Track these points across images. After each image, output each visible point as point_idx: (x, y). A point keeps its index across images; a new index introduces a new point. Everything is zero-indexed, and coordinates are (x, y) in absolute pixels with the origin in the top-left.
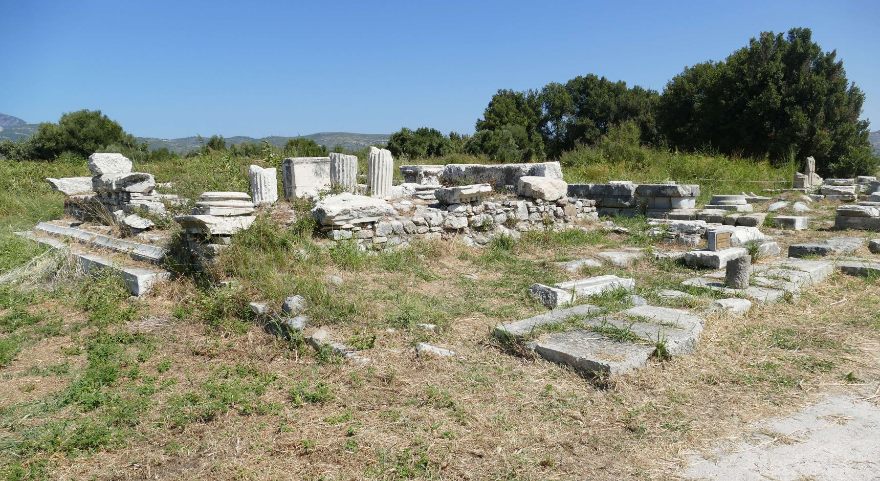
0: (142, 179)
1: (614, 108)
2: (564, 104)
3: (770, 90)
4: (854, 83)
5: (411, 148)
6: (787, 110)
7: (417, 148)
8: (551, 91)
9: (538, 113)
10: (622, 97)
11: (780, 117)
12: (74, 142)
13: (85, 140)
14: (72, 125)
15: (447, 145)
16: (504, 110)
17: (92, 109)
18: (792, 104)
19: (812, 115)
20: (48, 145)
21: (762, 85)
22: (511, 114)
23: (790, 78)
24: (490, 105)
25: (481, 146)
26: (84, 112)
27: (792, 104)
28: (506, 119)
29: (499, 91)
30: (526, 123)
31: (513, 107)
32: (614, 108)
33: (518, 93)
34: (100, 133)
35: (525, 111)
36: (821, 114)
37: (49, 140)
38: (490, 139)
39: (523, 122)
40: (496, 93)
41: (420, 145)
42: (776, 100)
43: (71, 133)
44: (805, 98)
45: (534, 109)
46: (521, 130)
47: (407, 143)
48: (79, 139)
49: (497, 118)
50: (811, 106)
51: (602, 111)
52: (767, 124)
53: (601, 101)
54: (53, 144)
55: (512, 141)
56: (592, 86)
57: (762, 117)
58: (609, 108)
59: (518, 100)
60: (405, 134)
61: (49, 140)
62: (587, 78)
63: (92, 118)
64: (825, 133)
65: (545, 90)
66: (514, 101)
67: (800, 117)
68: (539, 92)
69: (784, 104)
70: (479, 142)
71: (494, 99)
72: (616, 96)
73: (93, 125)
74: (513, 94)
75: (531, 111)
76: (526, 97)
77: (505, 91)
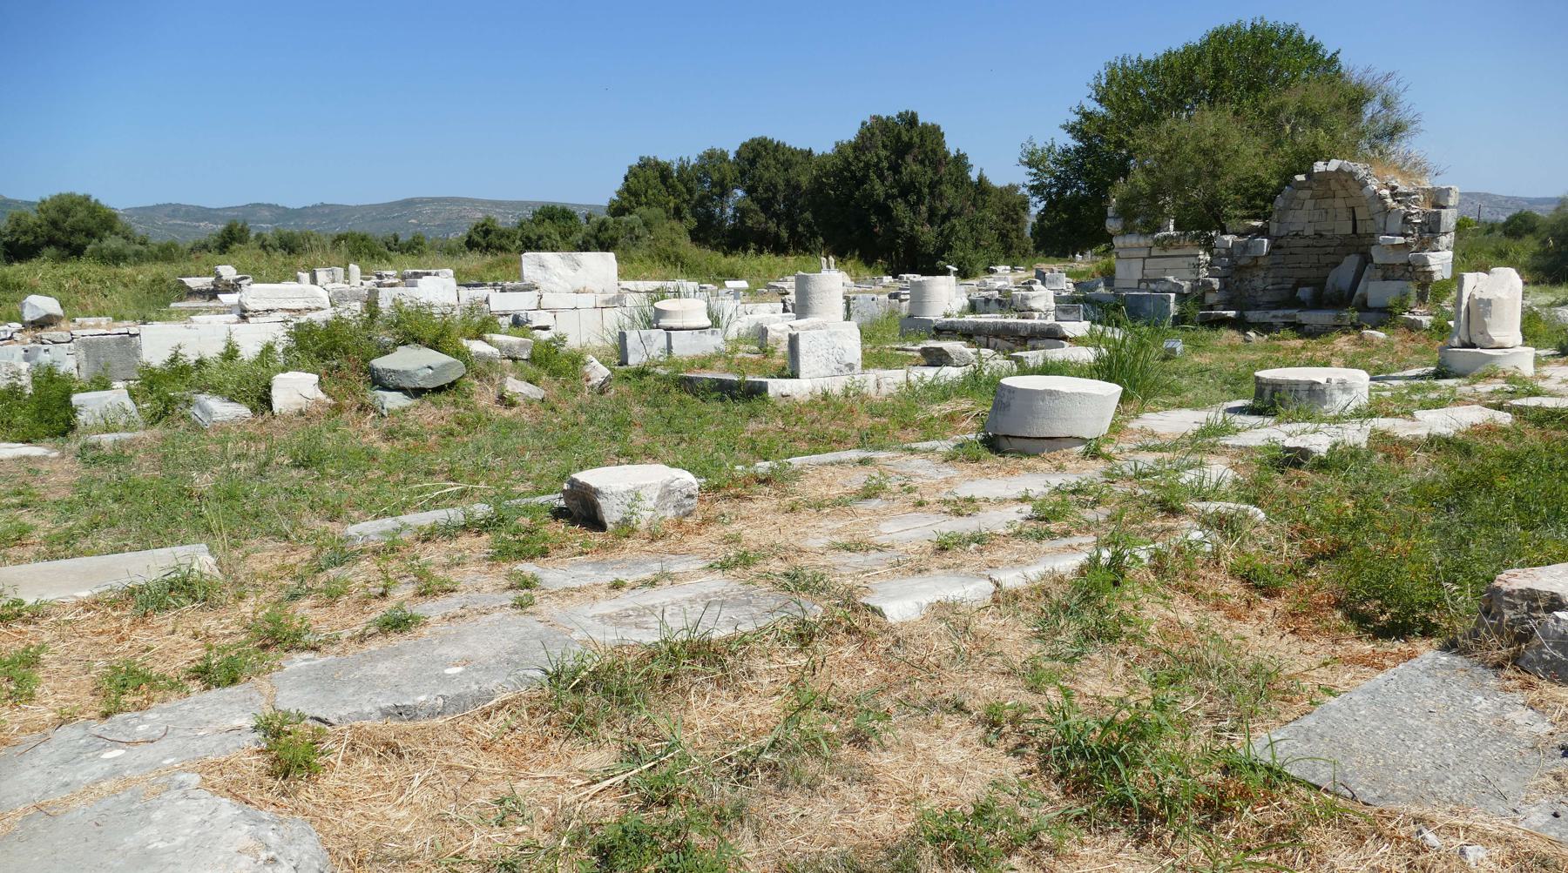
0: (246, 278)
2: (723, 179)
3: (872, 181)
4: (982, 170)
5: (498, 242)
11: (884, 211)
12: (58, 235)
13: (72, 233)
14: (53, 214)
15: (549, 237)
16: (643, 186)
17: (80, 192)
18: (893, 197)
19: (914, 207)
20: (23, 239)
21: (865, 178)
23: (895, 168)
25: (596, 237)
26: (70, 196)
27: (893, 197)
29: (641, 159)
30: (672, 205)
33: (665, 163)
34: (92, 223)
35: (673, 187)
36: (923, 209)
37: (25, 233)
38: (607, 229)
39: (668, 203)
40: (635, 162)
41: (508, 237)
42: (879, 190)
43: (54, 224)
44: (907, 190)
45: (685, 186)
47: (492, 236)
48: (64, 231)
49: (632, 198)
50: (913, 198)
51: (766, 190)
52: (874, 219)
53: (767, 175)
54: (30, 238)
57: (868, 210)
59: (664, 172)
60: (489, 223)
61: (25, 233)
63: (80, 204)
64: (927, 228)
65: (701, 157)
67: (900, 209)
69: (888, 196)
71: (630, 172)
72: (786, 170)
73: (81, 214)
74: (657, 164)
75: (681, 187)
76: (675, 168)
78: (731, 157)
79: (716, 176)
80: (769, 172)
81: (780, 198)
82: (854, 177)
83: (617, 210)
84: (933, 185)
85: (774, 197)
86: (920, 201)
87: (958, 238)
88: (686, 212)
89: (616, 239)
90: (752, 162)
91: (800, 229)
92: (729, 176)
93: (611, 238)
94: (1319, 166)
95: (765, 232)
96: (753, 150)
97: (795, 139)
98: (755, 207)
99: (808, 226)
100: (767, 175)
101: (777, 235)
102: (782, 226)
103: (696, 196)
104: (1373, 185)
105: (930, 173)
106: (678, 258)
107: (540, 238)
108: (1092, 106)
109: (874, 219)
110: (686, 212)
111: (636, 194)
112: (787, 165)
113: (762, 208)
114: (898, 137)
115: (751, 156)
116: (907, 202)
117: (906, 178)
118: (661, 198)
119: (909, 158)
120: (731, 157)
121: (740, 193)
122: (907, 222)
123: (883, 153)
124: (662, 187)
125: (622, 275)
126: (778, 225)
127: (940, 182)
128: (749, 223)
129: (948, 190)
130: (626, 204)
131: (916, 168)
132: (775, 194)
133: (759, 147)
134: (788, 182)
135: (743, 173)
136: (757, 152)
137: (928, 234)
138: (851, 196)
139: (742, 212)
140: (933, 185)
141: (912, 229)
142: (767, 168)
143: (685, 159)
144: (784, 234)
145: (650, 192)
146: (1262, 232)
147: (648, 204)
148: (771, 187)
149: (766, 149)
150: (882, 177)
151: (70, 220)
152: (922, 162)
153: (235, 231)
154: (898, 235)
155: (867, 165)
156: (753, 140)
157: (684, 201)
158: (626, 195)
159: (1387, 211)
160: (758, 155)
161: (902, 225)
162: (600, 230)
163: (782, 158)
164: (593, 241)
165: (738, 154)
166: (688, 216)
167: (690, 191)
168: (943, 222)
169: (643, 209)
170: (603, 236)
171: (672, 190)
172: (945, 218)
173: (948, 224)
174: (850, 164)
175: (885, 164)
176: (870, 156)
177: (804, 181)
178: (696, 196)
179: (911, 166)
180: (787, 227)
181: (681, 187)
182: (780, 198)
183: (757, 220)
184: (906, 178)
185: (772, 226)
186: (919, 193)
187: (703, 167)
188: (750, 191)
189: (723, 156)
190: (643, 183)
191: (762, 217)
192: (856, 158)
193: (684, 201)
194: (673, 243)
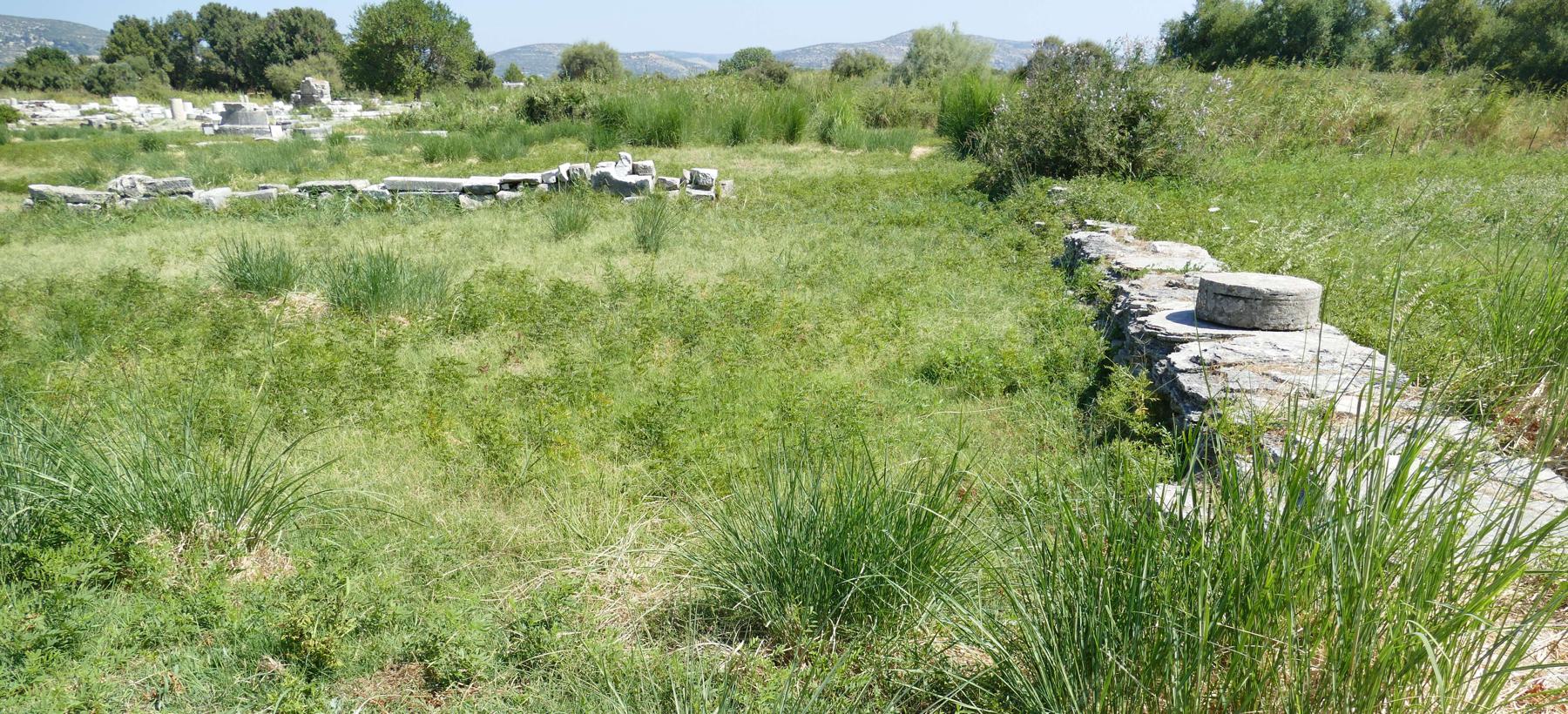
2: (190, 35)
7: (32, 82)
8: (180, 18)
23: (290, 42)
25: (97, 78)
30: (152, 53)
32: (234, 42)
35: (150, 39)
38: (105, 73)
39: (149, 52)
51: (223, 45)
58: (229, 43)
59: (142, 28)
68: (164, 22)
70: (96, 74)
71: (115, 27)
72: (236, 30)
74: (137, 21)
78: (195, 18)
79: (184, 33)
80: (223, 31)
82: (266, 47)
85: (229, 50)
88: (165, 59)
89: (114, 80)
90: (212, 22)
92: (195, 32)
98: (216, 57)
102: (239, 71)
103: (170, 47)
106: (158, 94)
110: (165, 59)
111: (122, 45)
112: (236, 27)
113: (221, 57)
114: (289, 24)
115: (210, 17)
117: (297, 49)
118: (142, 48)
119: (298, 36)
120: (195, 18)
121: (205, 44)
123: (281, 33)
124: (142, 40)
126: (235, 70)
130: (115, 52)
131: (301, 42)
132: (230, 48)
133: (215, 12)
135: (205, 30)
139: (207, 61)
145: (133, 44)
147: (133, 53)
149: (221, 12)
150: (282, 47)
152: (306, 39)
155: (272, 40)
156: (210, 4)
158: (114, 45)
160: (215, 16)
162: (100, 73)
163: (233, 20)
165: (200, 15)
166: (167, 62)
167: (165, 43)
169: (129, 57)
170: (103, 78)
171: (150, 42)
175: (283, 40)
176: (272, 35)
178: (170, 47)
179: (299, 42)
180: (243, 72)
181: (157, 40)
183: (218, 66)
185: (231, 71)
187: (173, 24)
188: (213, 43)
189: (188, 16)
190: (127, 37)
191: (222, 64)
194: (155, 87)
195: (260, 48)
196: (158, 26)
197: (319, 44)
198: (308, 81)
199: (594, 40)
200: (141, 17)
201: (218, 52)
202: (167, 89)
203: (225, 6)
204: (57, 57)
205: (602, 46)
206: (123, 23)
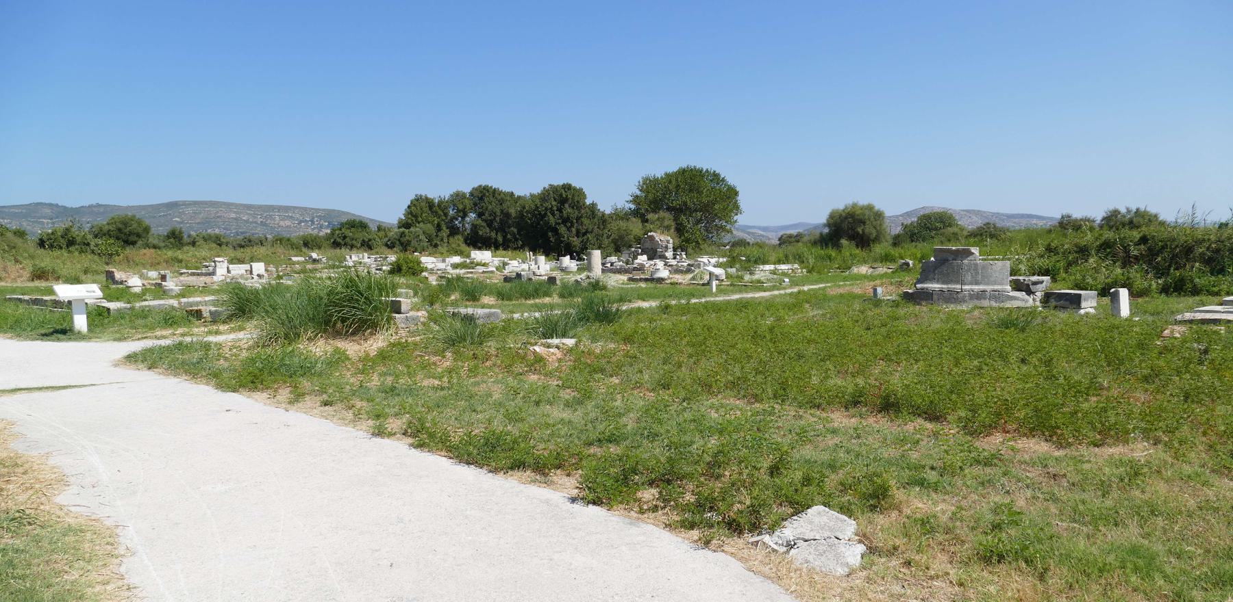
1: (498, 214)
6: (557, 226)
7: (354, 242)
8: (458, 196)
9: (446, 215)
10: (505, 206)
11: (555, 231)
13: (129, 235)
16: (419, 212)
18: (559, 224)
19: (569, 229)
21: (546, 214)
22: (424, 215)
23: (560, 210)
24: (409, 207)
25: (399, 240)
27: (559, 224)
28: (420, 219)
29: (416, 196)
30: (436, 222)
31: (426, 209)
32: (498, 214)
34: (140, 230)
35: (436, 212)
38: (405, 236)
39: (434, 221)
40: (413, 197)
41: (356, 240)
44: (565, 221)
45: (443, 211)
46: (430, 228)
47: (347, 239)
48: (125, 234)
51: (490, 215)
52: (550, 234)
53: (490, 207)
55: (422, 237)
56: (487, 194)
59: (430, 204)
62: (484, 188)
65: (452, 196)
66: (427, 205)
67: (562, 229)
68: (446, 199)
69: (557, 224)
71: (411, 203)
72: (501, 204)
73: (135, 226)
74: (427, 198)
75: (440, 213)
76: (437, 201)
77: (421, 196)
80: (493, 206)
81: (498, 219)
82: (540, 214)
83: (405, 225)
84: (578, 219)
85: (495, 219)
86: (572, 226)
87: (590, 244)
90: (481, 199)
91: (509, 236)
93: (408, 241)
94: (649, 234)
95: (490, 238)
96: (481, 192)
97: (504, 186)
98: (484, 224)
99: (513, 235)
100: (490, 207)
101: (496, 239)
104: (657, 239)
105: (577, 212)
107: (370, 240)
108: (638, 193)
109: (550, 234)
111: (416, 217)
112: (501, 202)
114: (561, 195)
115: (480, 195)
116: (565, 226)
117: (565, 215)
119: (567, 205)
122: (565, 235)
123: (554, 203)
125: (492, 257)
127: (581, 217)
128: (481, 233)
129: (586, 221)
130: (410, 221)
131: (570, 210)
134: (502, 211)
135: (475, 205)
136: (483, 195)
137: (576, 241)
138: (539, 224)
139: (475, 227)
140: (578, 219)
141: (569, 239)
142: (490, 203)
143: (442, 197)
144: (500, 239)
146: (640, 248)
148: (493, 214)
149: (488, 191)
150: (553, 215)
151: (128, 229)
152: (573, 207)
153: (177, 233)
154: (562, 242)
155: (546, 209)
156: (480, 186)
157: (443, 220)
158: (410, 216)
159: (659, 244)
160: (484, 195)
161: (564, 237)
162: (401, 237)
163: (499, 198)
164: (398, 242)
166: (444, 228)
168: (583, 236)
169: (422, 225)
170: (403, 240)
172: (585, 234)
173: (585, 237)
174: (538, 207)
175: (555, 208)
176: (547, 205)
177: (512, 211)
179: (567, 210)
182: (498, 219)
183: (484, 231)
184: (565, 215)
185: (493, 234)
186: (572, 222)
188: (480, 215)
189: (464, 195)
191: (488, 230)
192: (542, 205)
193: (443, 220)
195: (534, 215)
196: (441, 202)
197: (583, 211)
198: (652, 238)
199: (863, 201)
200: (430, 196)
201: (485, 221)
202: (464, 247)
203: (491, 187)
204: (361, 226)
205: (870, 208)
206: (417, 200)
